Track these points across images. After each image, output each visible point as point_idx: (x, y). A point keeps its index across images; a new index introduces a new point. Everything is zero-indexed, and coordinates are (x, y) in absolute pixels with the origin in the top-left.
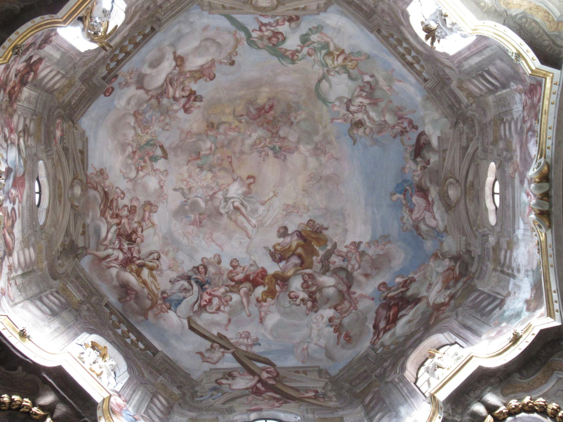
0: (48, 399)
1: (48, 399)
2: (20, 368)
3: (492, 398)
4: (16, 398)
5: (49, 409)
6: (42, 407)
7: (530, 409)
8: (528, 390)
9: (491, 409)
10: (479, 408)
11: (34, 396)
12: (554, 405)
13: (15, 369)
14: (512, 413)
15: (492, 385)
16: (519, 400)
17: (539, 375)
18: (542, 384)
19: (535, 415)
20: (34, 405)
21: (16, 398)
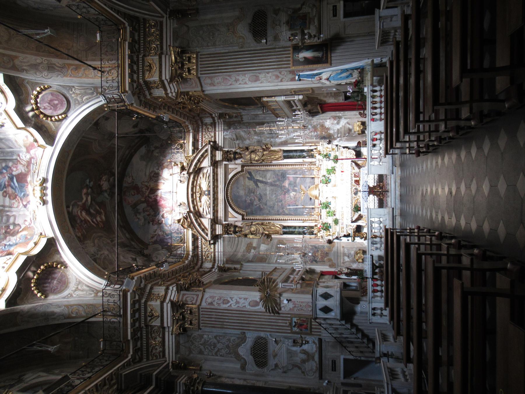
0: (30, 274)
1: (30, 274)
2: (20, 287)
3: (28, 108)
4: (32, 285)
5: (34, 273)
6: (34, 275)
7: (37, 97)
8: (28, 95)
9: (33, 110)
10: (31, 114)
11: (30, 279)
12: (38, 89)
13: (21, 288)
14: (36, 103)
15: (22, 107)
16: (32, 99)
17: (23, 89)
18: (27, 89)
19: (40, 96)
20: (33, 278)
21: (32, 285)
